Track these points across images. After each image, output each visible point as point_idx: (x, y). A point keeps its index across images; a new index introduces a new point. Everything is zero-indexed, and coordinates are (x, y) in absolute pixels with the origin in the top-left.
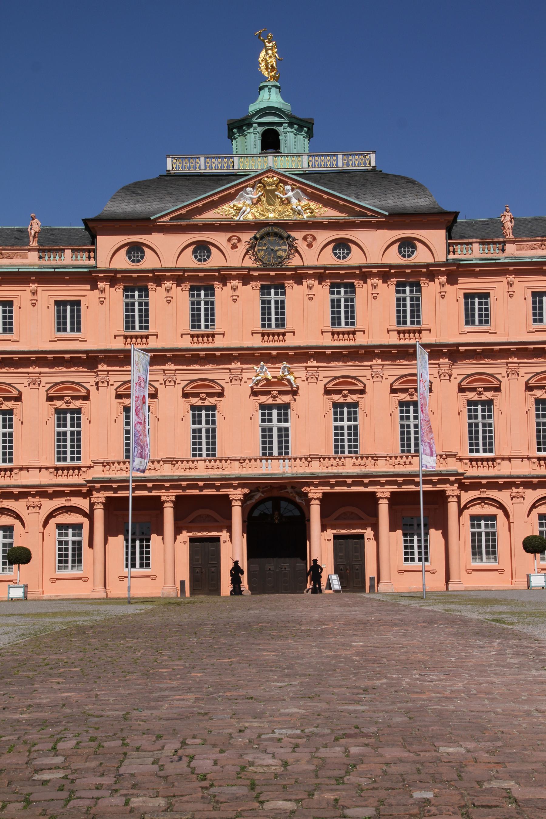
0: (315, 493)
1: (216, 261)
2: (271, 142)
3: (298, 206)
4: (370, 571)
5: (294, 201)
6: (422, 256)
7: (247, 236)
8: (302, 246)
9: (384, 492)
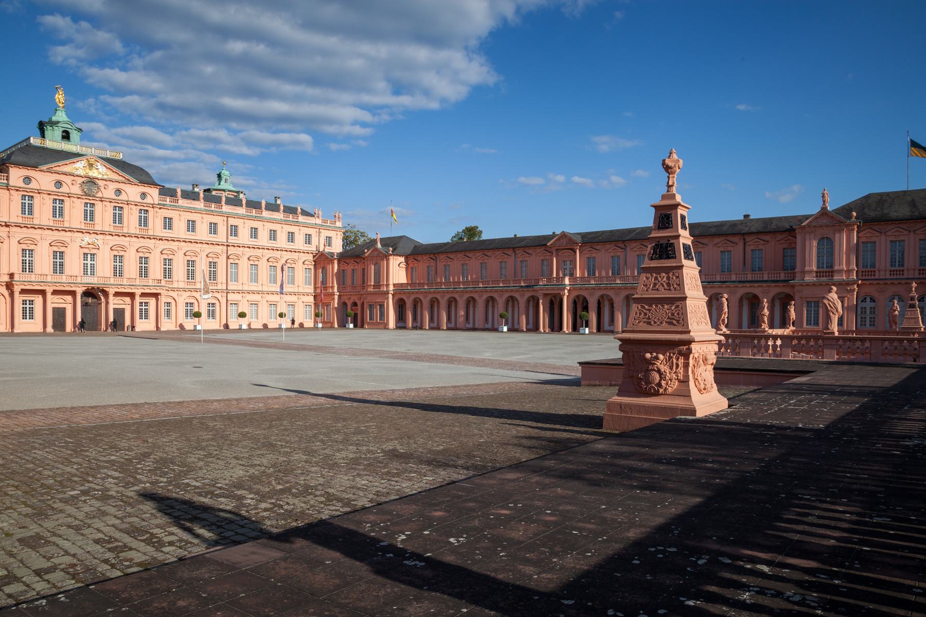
0: (111, 291)
1: (65, 189)
2: (66, 136)
3: (101, 171)
4: (128, 322)
5: (100, 170)
6: (149, 200)
7: (80, 180)
8: (102, 188)
9: (138, 292)
